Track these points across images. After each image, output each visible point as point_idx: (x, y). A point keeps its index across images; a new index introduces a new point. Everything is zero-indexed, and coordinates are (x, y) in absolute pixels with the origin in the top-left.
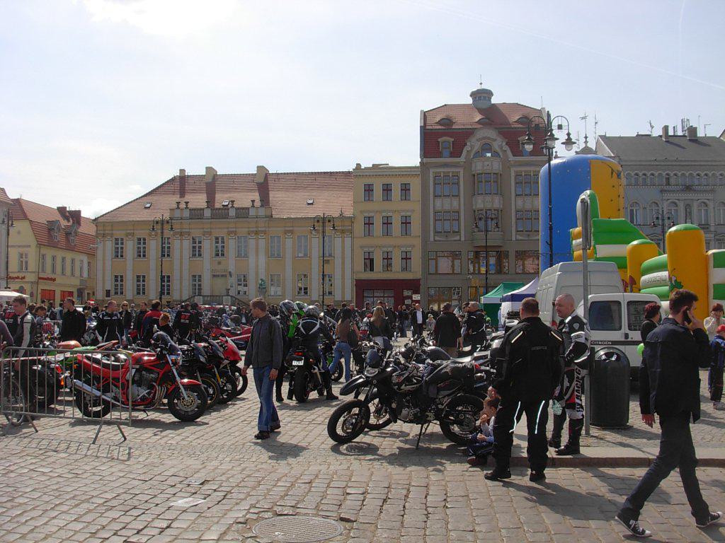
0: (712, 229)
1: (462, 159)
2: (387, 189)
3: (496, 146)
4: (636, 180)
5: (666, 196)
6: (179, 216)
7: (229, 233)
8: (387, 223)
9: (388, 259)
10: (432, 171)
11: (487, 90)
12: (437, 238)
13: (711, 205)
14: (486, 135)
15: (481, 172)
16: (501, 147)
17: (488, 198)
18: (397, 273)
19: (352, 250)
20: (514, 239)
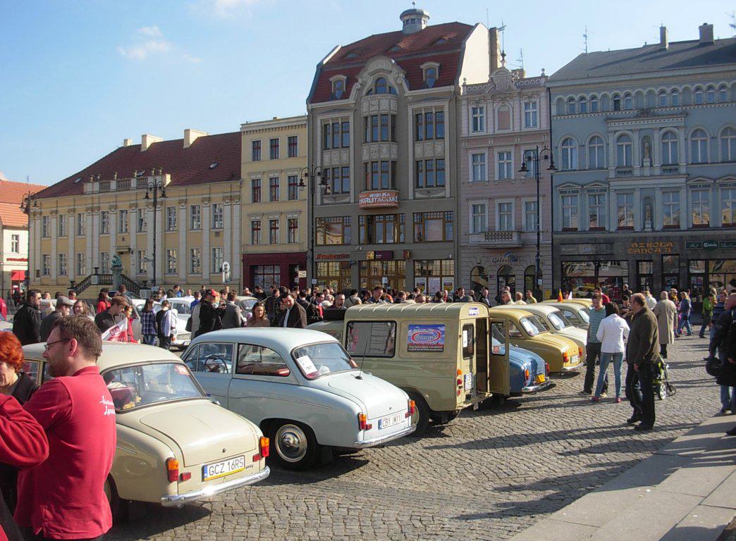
0: (683, 170)
1: (351, 100)
2: (274, 144)
3: (391, 79)
4: (572, 107)
5: (614, 126)
6: (91, 190)
7: (180, 202)
8: (274, 186)
9: (273, 226)
10: (319, 119)
11: (406, 11)
12: (326, 201)
13: (681, 134)
14: (380, 67)
15: (375, 113)
16: (396, 79)
17: (374, 147)
18: (282, 247)
19: (241, 219)
20: (411, 197)
